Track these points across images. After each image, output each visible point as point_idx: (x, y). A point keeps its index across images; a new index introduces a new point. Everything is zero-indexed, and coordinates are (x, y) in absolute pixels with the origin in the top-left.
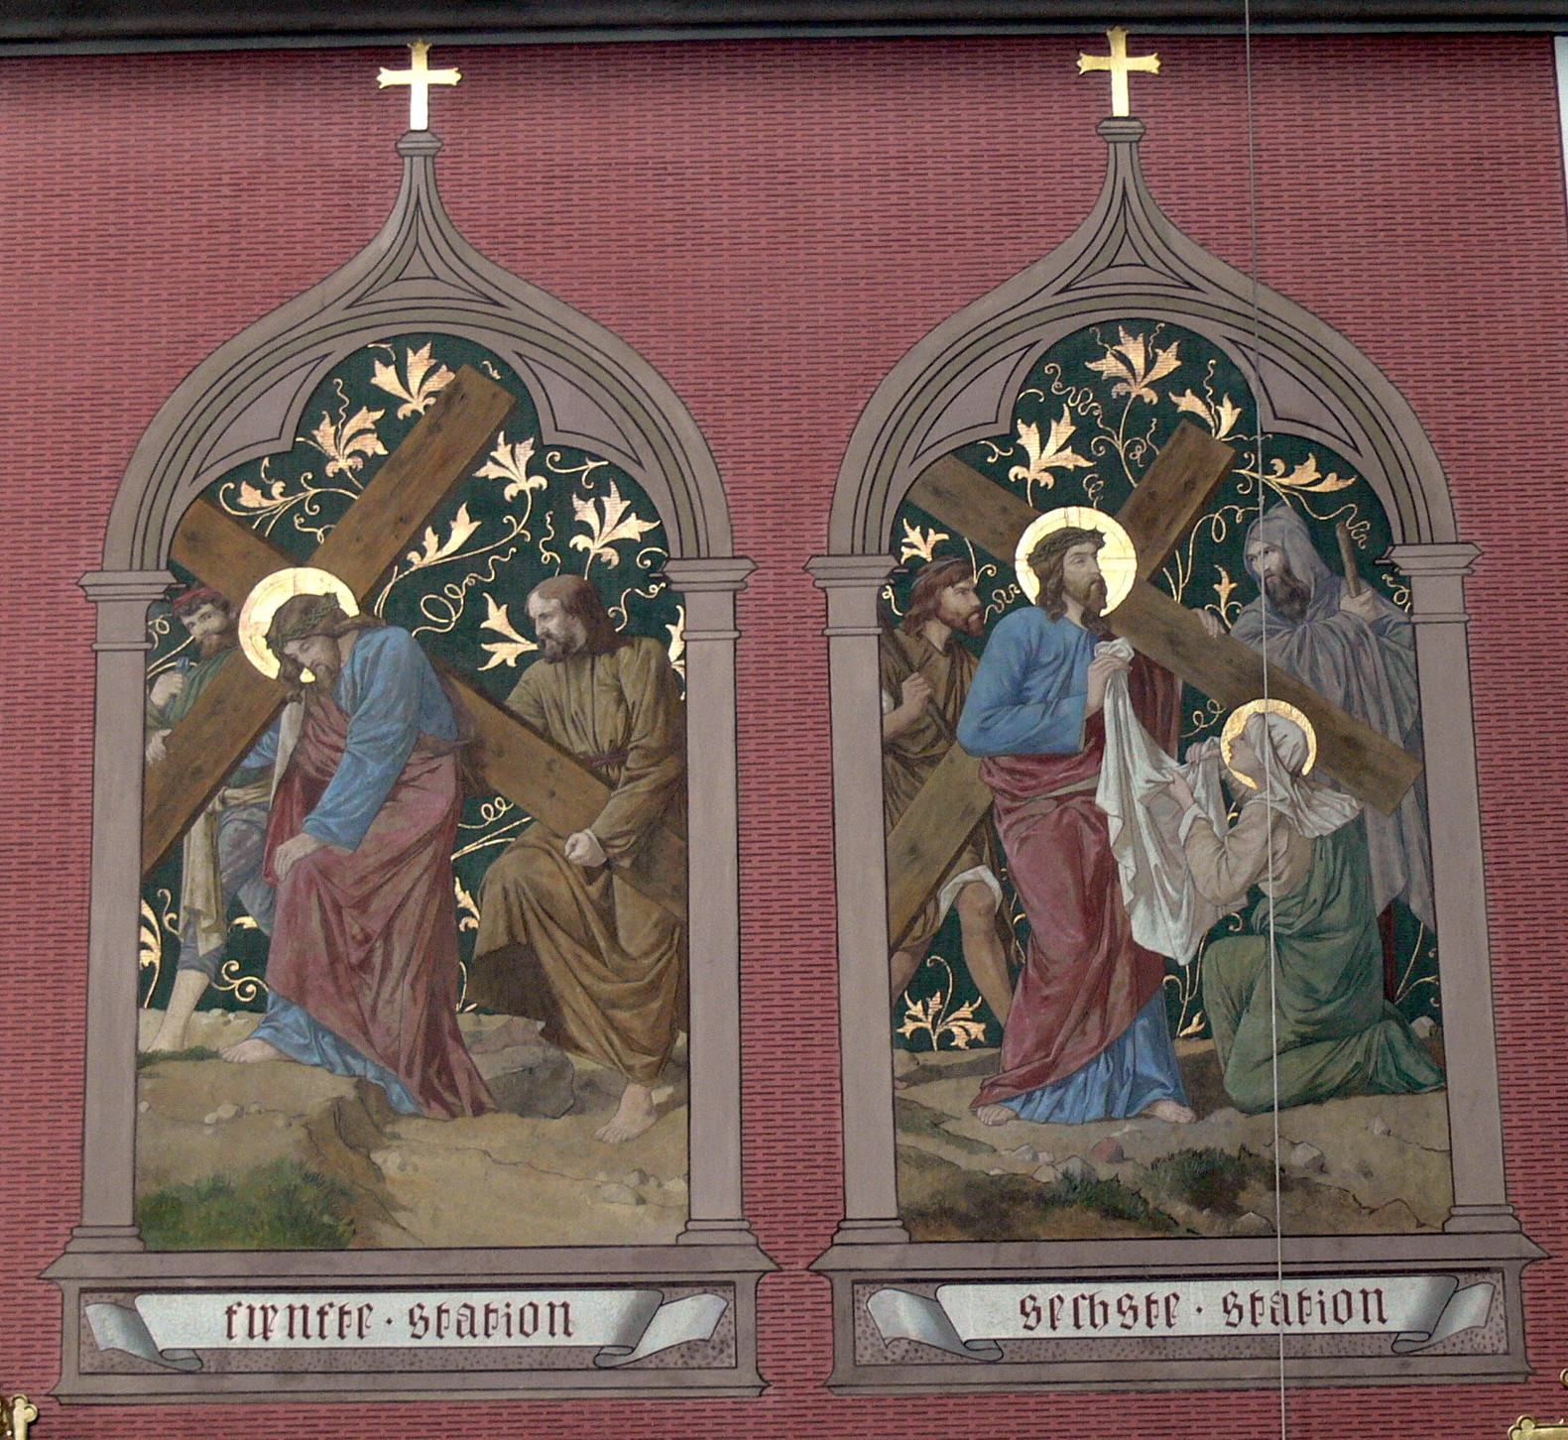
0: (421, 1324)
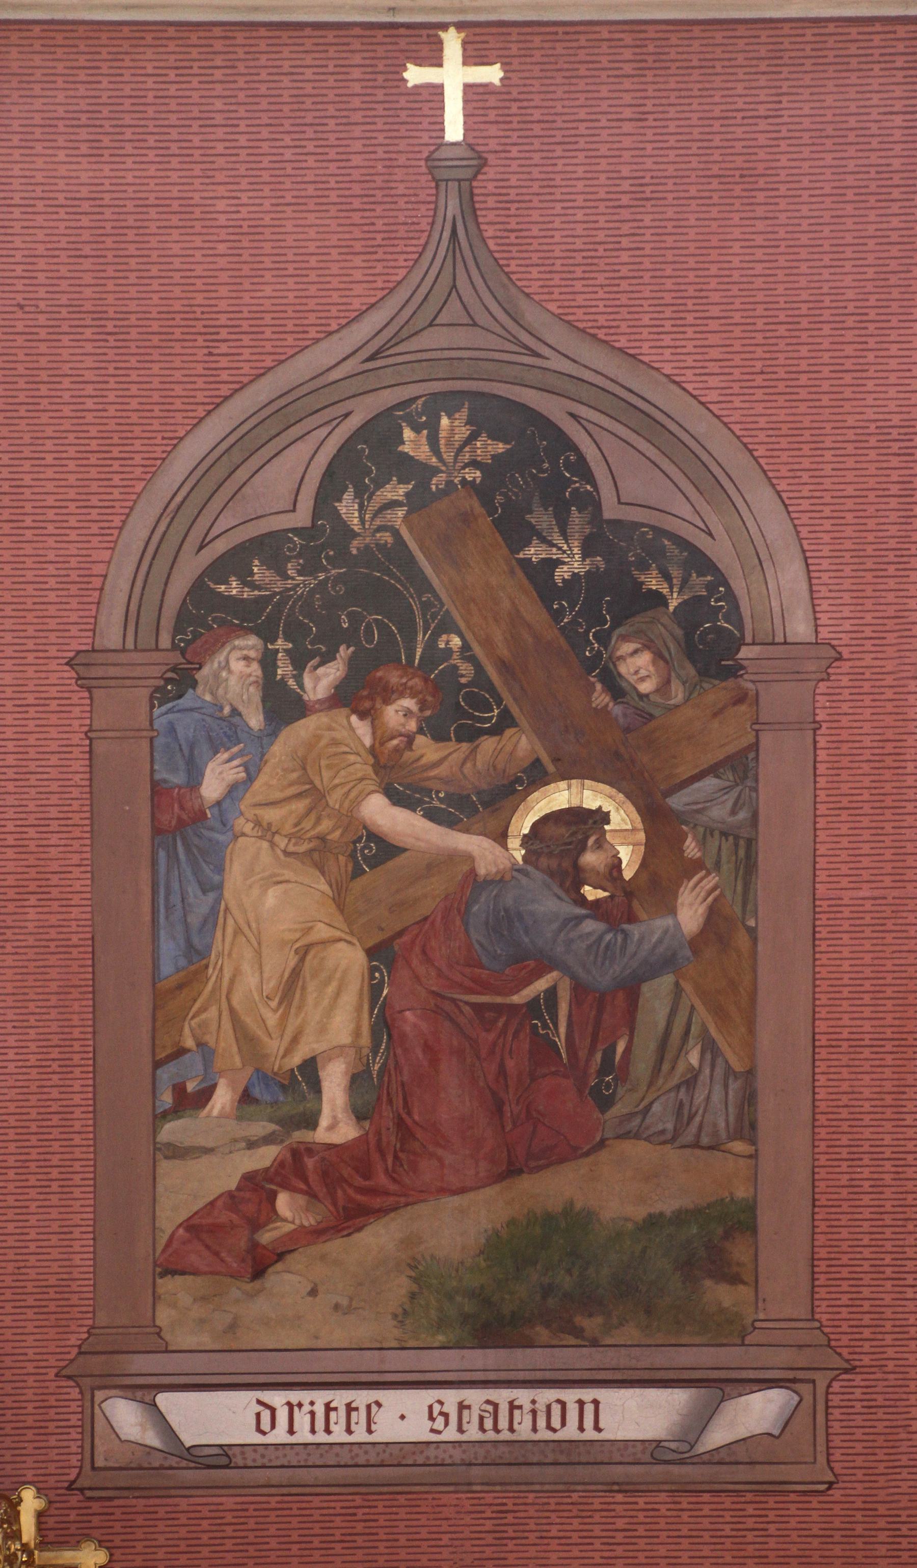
0: (440, 1420)
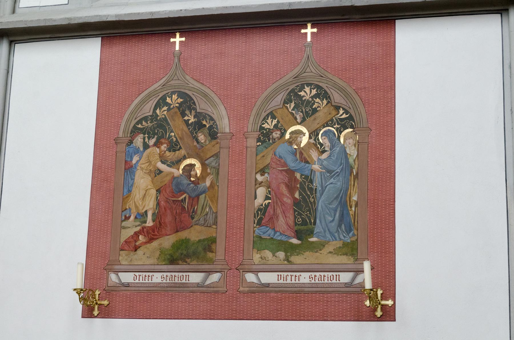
0: (311, 279)
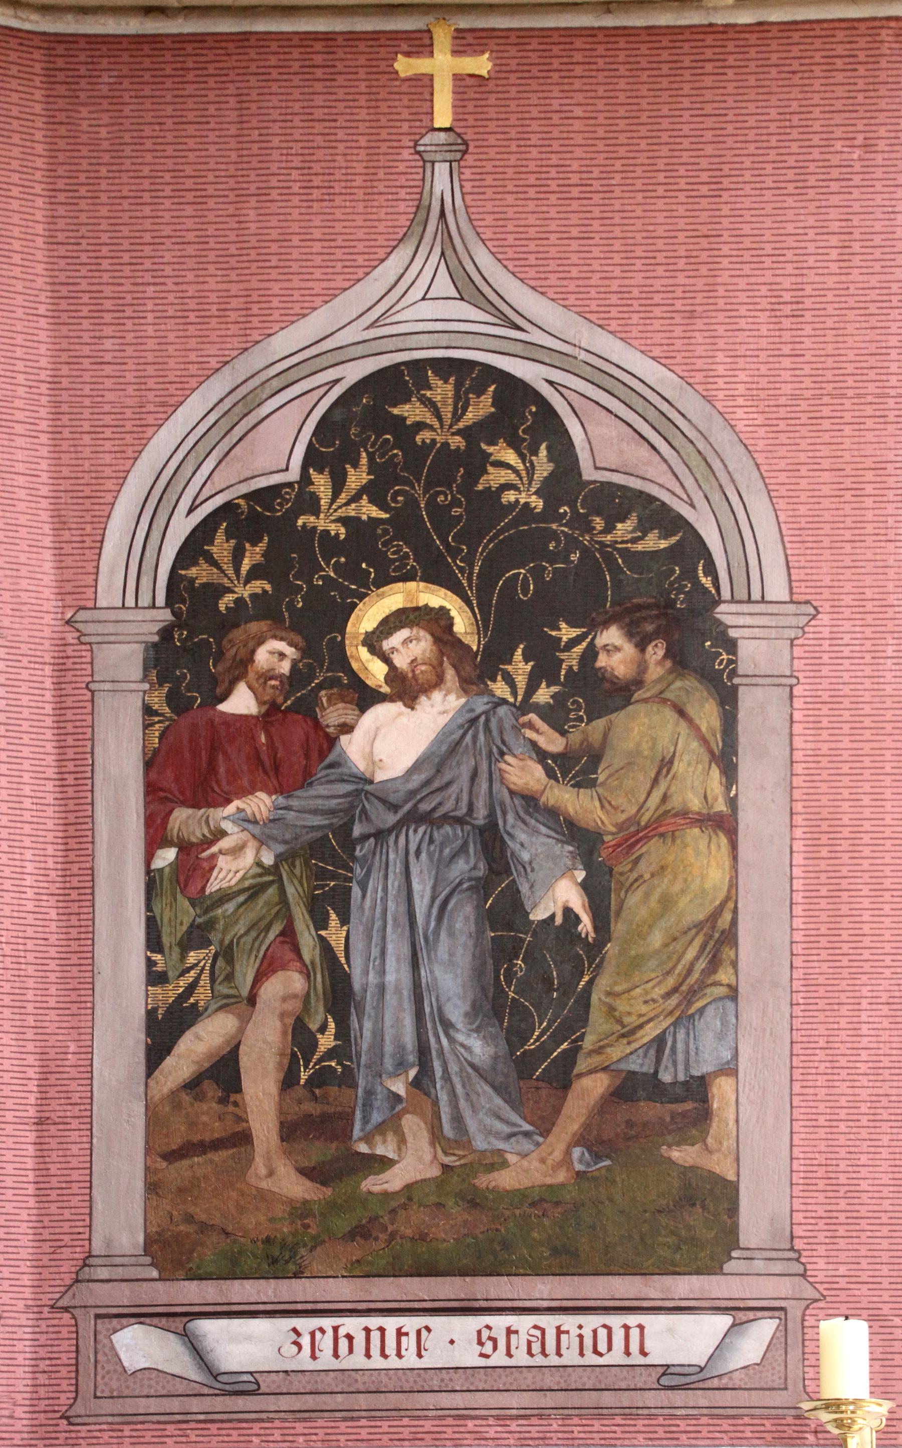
0: (489, 1345)
